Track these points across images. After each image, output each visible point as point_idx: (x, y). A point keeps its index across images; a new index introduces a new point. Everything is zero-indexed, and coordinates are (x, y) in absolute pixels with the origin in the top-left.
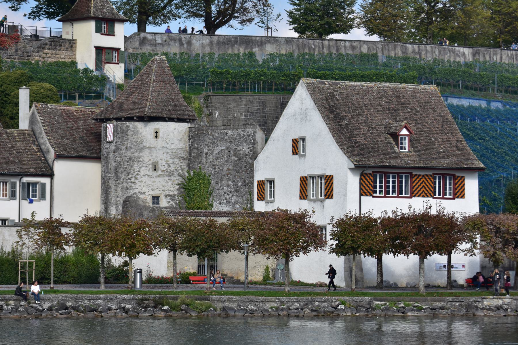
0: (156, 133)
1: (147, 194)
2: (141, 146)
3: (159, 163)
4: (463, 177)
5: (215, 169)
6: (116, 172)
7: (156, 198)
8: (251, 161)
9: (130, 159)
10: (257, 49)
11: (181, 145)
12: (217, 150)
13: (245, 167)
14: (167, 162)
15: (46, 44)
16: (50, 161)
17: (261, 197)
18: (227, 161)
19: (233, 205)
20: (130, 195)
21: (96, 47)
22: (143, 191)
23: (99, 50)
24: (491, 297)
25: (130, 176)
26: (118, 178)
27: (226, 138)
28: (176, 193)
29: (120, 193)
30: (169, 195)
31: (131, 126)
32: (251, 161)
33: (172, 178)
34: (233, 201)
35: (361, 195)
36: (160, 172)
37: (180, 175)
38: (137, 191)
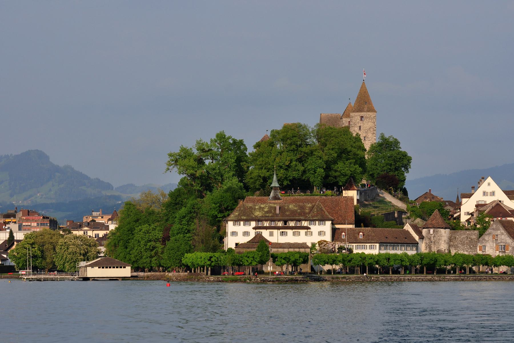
6: (434, 242)
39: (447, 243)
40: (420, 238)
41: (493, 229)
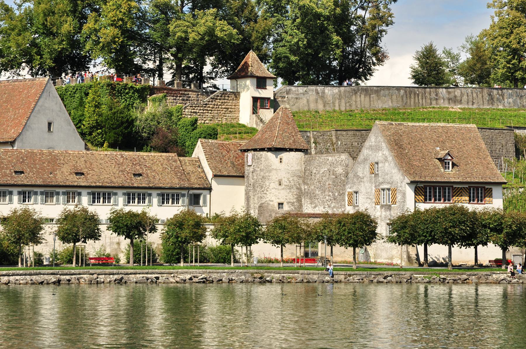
0: (281, 159)
1: (275, 201)
2: (270, 168)
3: (283, 179)
4: (491, 188)
5: (320, 184)
7: (281, 204)
8: (343, 178)
9: (263, 177)
10: (374, 95)
11: (299, 168)
12: (322, 171)
13: (340, 182)
14: (288, 179)
15: (218, 96)
16: (210, 179)
17: (350, 203)
18: (328, 179)
19: (333, 209)
20: (263, 202)
21: (253, 97)
22: (272, 199)
23: (255, 100)
24: (498, 272)
25: (263, 189)
26: (255, 190)
27: (328, 162)
28: (295, 200)
29: (256, 201)
30: (290, 202)
31: (263, 154)
32: (343, 178)
33: (292, 190)
34: (332, 206)
35: (415, 202)
36: (283, 187)
37: (298, 188)
38: (267, 199)
39: (290, 188)
40: (215, 176)
41: (371, 148)
